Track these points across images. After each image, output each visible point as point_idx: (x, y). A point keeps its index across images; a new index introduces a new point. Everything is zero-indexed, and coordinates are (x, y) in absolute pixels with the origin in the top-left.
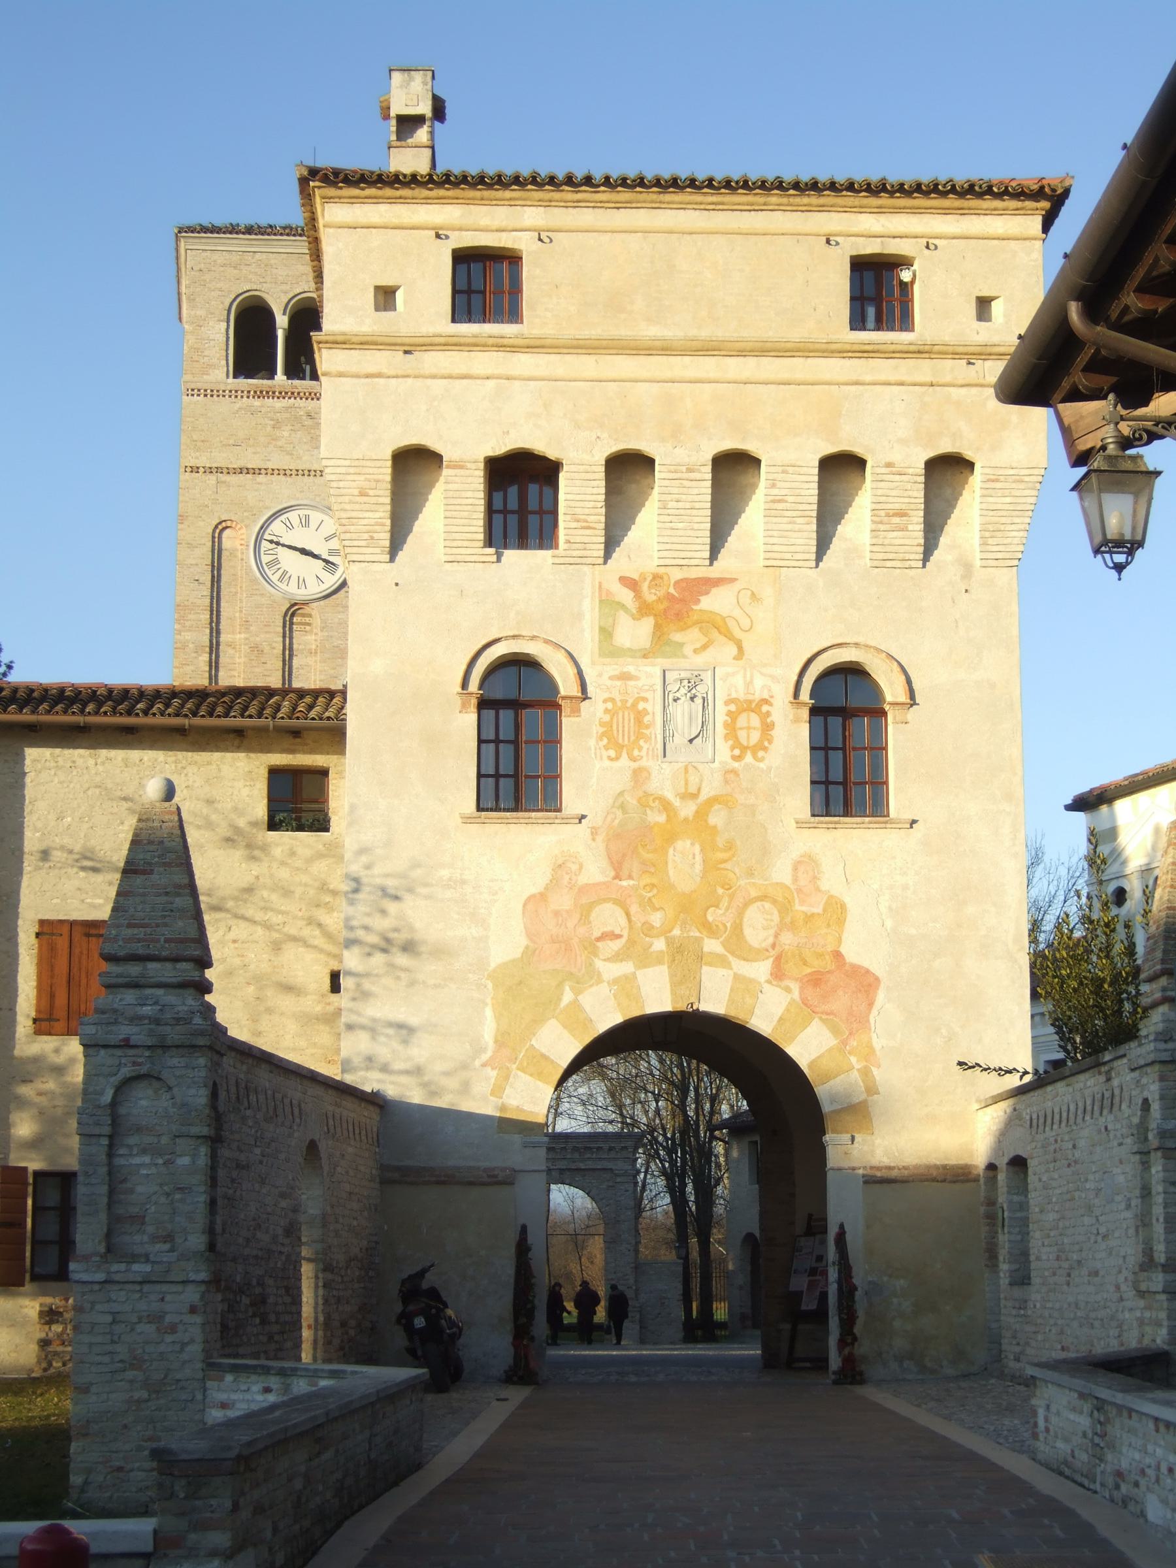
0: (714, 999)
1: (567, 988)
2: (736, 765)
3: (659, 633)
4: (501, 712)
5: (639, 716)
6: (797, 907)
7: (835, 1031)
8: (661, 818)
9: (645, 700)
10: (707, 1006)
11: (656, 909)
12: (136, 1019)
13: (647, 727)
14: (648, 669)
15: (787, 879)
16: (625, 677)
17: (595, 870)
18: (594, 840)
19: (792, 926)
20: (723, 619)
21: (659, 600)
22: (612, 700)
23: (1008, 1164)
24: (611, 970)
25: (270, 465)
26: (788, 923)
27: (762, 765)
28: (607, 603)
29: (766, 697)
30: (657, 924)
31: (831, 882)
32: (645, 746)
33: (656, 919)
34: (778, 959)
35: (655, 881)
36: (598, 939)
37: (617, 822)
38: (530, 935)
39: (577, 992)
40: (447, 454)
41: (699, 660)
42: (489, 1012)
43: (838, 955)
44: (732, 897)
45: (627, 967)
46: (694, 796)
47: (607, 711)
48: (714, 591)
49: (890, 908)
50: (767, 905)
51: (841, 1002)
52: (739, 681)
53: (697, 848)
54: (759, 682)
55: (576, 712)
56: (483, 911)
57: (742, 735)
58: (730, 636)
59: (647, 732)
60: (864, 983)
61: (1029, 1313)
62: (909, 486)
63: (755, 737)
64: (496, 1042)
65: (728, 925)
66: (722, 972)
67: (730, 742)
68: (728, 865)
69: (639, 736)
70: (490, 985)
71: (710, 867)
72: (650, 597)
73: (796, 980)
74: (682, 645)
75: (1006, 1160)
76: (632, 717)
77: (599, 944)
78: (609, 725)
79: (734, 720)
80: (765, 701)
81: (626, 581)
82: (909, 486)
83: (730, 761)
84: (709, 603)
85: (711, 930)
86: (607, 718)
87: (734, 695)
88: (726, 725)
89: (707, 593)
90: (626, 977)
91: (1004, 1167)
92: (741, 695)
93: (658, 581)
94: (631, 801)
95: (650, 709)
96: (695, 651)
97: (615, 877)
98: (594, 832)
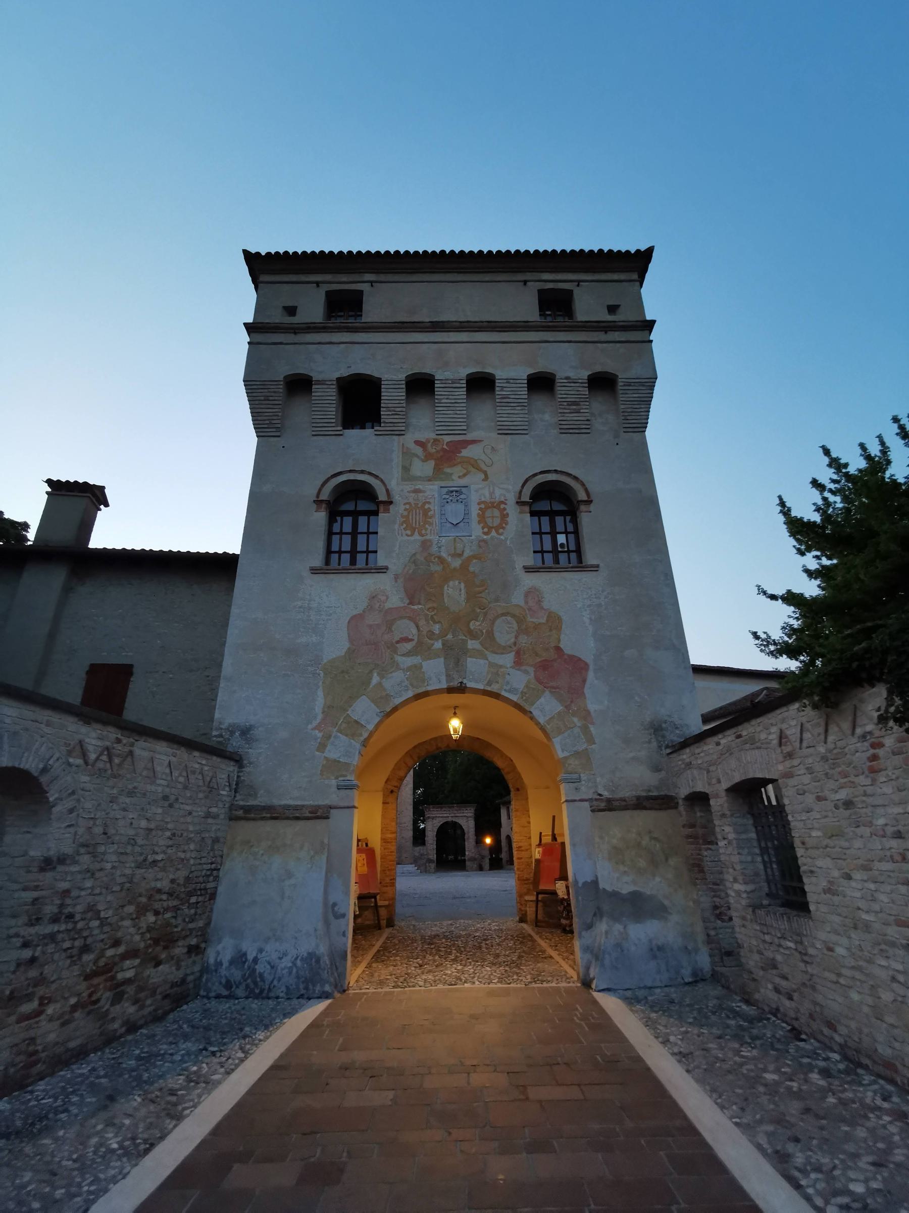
3: (438, 470)
4: (345, 518)
5: (426, 513)
6: (529, 619)
9: (429, 503)
11: (435, 622)
13: (430, 518)
14: (431, 487)
15: (522, 603)
16: (417, 491)
17: (396, 600)
18: (396, 581)
21: (437, 452)
22: (409, 503)
23: (729, 790)
26: (523, 628)
27: (502, 537)
28: (406, 453)
29: (502, 499)
30: (437, 632)
31: (551, 602)
32: (429, 528)
33: (436, 629)
34: (518, 653)
35: (435, 605)
36: (398, 642)
37: (411, 571)
38: (351, 640)
39: (382, 677)
40: (316, 376)
41: (462, 482)
42: (320, 693)
43: (558, 649)
44: (485, 614)
46: (460, 555)
47: (406, 509)
48: (470, 447)
49: (591, 619)
50: (509, 618)
53: (462, 585)
57: (489, 521)
60: (578, 666)
61: (811, 951)
62: (580, 389)
66: (482, 662)
68: (483, 595)
69: (426, 522)
70: (322, 675)
72: (432, 450)
73: (532, 666)
75: (726, 785)
78: (408, 516)
79: (484, 513)
81: (417, 443)
82: (580, 389)
84: (465, 453)
85: (473, 635)
86: (405, 513)
88: (478, 515)
89: (465, 448)
90: (415, 666)
91: (723, 794)
96: (459, 477)
97: (411, 603)
98: (396, 577)
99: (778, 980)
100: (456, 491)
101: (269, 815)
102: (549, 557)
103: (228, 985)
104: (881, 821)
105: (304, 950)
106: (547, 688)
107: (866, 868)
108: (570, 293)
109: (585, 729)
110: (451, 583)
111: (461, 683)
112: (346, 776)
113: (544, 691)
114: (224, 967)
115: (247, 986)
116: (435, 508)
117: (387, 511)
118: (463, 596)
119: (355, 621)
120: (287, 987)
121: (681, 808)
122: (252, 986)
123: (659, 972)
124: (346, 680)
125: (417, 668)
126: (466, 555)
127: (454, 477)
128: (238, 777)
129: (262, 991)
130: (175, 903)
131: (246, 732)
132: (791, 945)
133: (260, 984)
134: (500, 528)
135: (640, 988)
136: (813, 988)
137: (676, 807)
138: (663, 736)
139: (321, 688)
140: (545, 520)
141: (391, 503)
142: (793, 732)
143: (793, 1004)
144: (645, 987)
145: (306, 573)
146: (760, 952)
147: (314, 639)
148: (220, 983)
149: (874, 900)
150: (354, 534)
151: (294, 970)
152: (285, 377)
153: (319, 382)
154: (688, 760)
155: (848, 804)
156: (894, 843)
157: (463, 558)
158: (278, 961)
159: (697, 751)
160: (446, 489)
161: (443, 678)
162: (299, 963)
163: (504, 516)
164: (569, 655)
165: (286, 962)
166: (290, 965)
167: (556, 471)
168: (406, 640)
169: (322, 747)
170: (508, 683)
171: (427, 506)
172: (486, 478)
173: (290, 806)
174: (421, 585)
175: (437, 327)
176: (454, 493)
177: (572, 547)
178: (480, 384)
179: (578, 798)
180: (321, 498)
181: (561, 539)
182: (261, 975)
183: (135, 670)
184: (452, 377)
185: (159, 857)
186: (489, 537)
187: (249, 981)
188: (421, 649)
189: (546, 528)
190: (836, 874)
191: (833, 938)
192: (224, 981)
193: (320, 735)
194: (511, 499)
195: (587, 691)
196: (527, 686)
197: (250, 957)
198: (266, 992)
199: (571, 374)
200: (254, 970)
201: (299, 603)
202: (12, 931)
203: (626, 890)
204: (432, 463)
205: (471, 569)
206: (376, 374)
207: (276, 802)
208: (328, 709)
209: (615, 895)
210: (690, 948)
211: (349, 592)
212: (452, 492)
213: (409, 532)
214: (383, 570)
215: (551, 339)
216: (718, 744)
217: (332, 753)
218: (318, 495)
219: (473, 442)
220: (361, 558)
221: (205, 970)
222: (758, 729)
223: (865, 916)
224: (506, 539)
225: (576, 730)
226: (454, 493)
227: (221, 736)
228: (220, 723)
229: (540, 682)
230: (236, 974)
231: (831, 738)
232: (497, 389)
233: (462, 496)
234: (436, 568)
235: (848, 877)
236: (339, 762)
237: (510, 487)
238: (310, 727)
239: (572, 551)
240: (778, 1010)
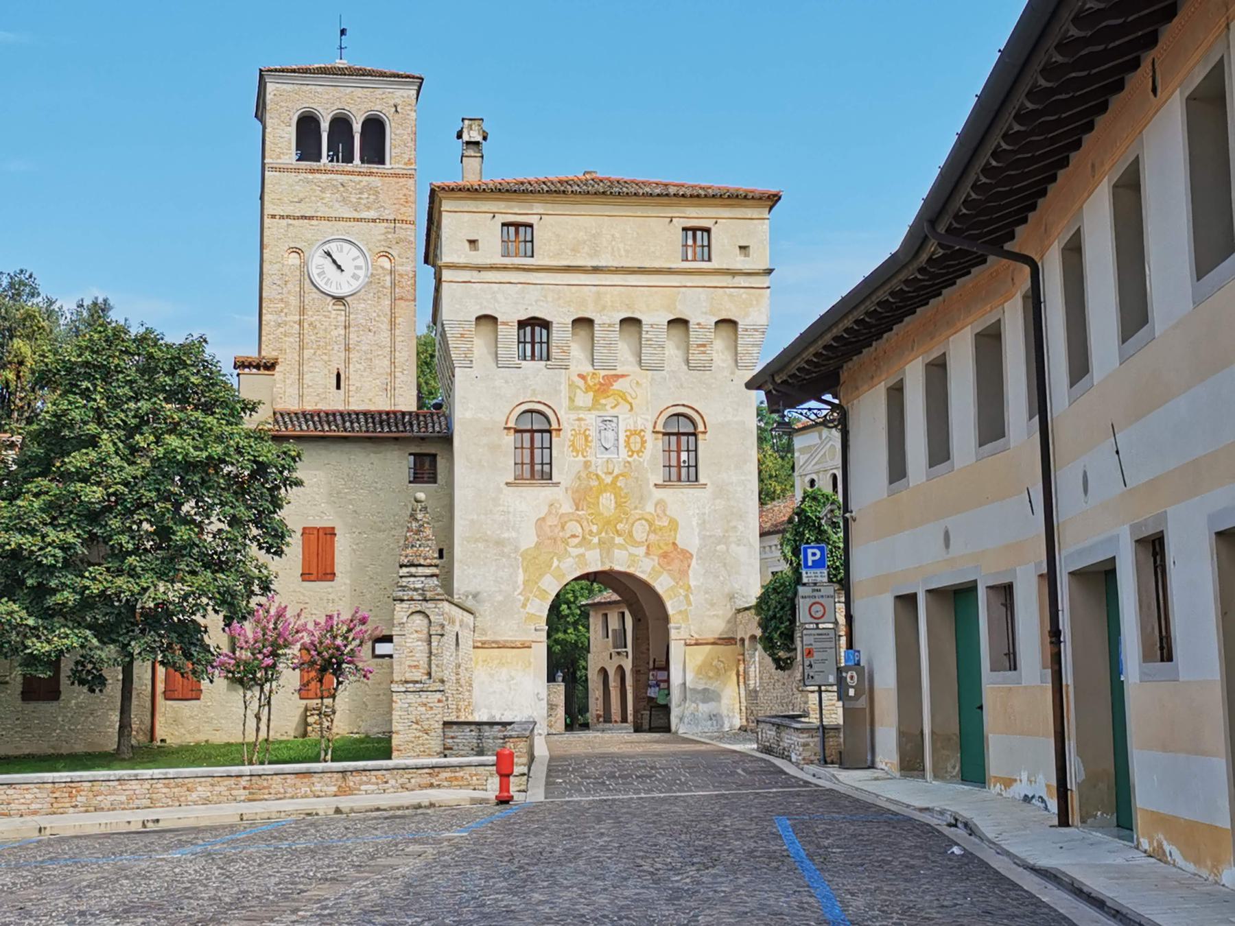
3: (595, 401)
5: (586, 437)
7: (674, 579)
10: (617, 568)
12: (415, 590)
16: (579, 420)
17: (567, 507)
19: (654, 532)
24: (575, 552)
25: (319, 214)
26: (653, 529)
28: (572, 386)
31: (673, 510)
33: (594, 528)
34: (648, 547)
42: (521, 570)
43: (674, 544)
45: (582, 550)
51: (676, 565)
52: (631, 421)
54: (640, 421)
55: (559, 436)
57: (632, 446)
58: (626, 400)
60: (686, 555)
63: (639, 446)
71: (618, 505)
72: (590, 383)
81: (579, 376)
85: (619, 534)
94: (583, 475)
97: (577, 509)
98: (567, 489)
109: (687, 596)
116: (593, 433)
117: (559, 436)
124: (535, 562)
125: (583, 555)
131: (475, 596)
140: (674, 438)
145: (503, 485)
147: (514, 534)
150: (532, 448)
153: (504, 323)
163: (643, 442)
168: (574, 536)
169: (524, 606)
172: (632, 409)
174: (583, 496)
175: (596, 270)
177: (692, 463)
180: (510, 425)
181: (684, 456)
188: (584, 542)
189: (673, 447)
193: (522, 598)
194: (650, 428)
195: (691, 573)
196: (653, 568)
199: (701, 321)
201: (501, 508)
203: (700, 687)
204: (591, 394)
206: (548, 318)
207: (498, 638)
208: (526, 582)
209: (694, 690)
211: (535, 498)
217: (530, 609)
219: (623, 376)
233: (614, 425)
234: (594, 483)
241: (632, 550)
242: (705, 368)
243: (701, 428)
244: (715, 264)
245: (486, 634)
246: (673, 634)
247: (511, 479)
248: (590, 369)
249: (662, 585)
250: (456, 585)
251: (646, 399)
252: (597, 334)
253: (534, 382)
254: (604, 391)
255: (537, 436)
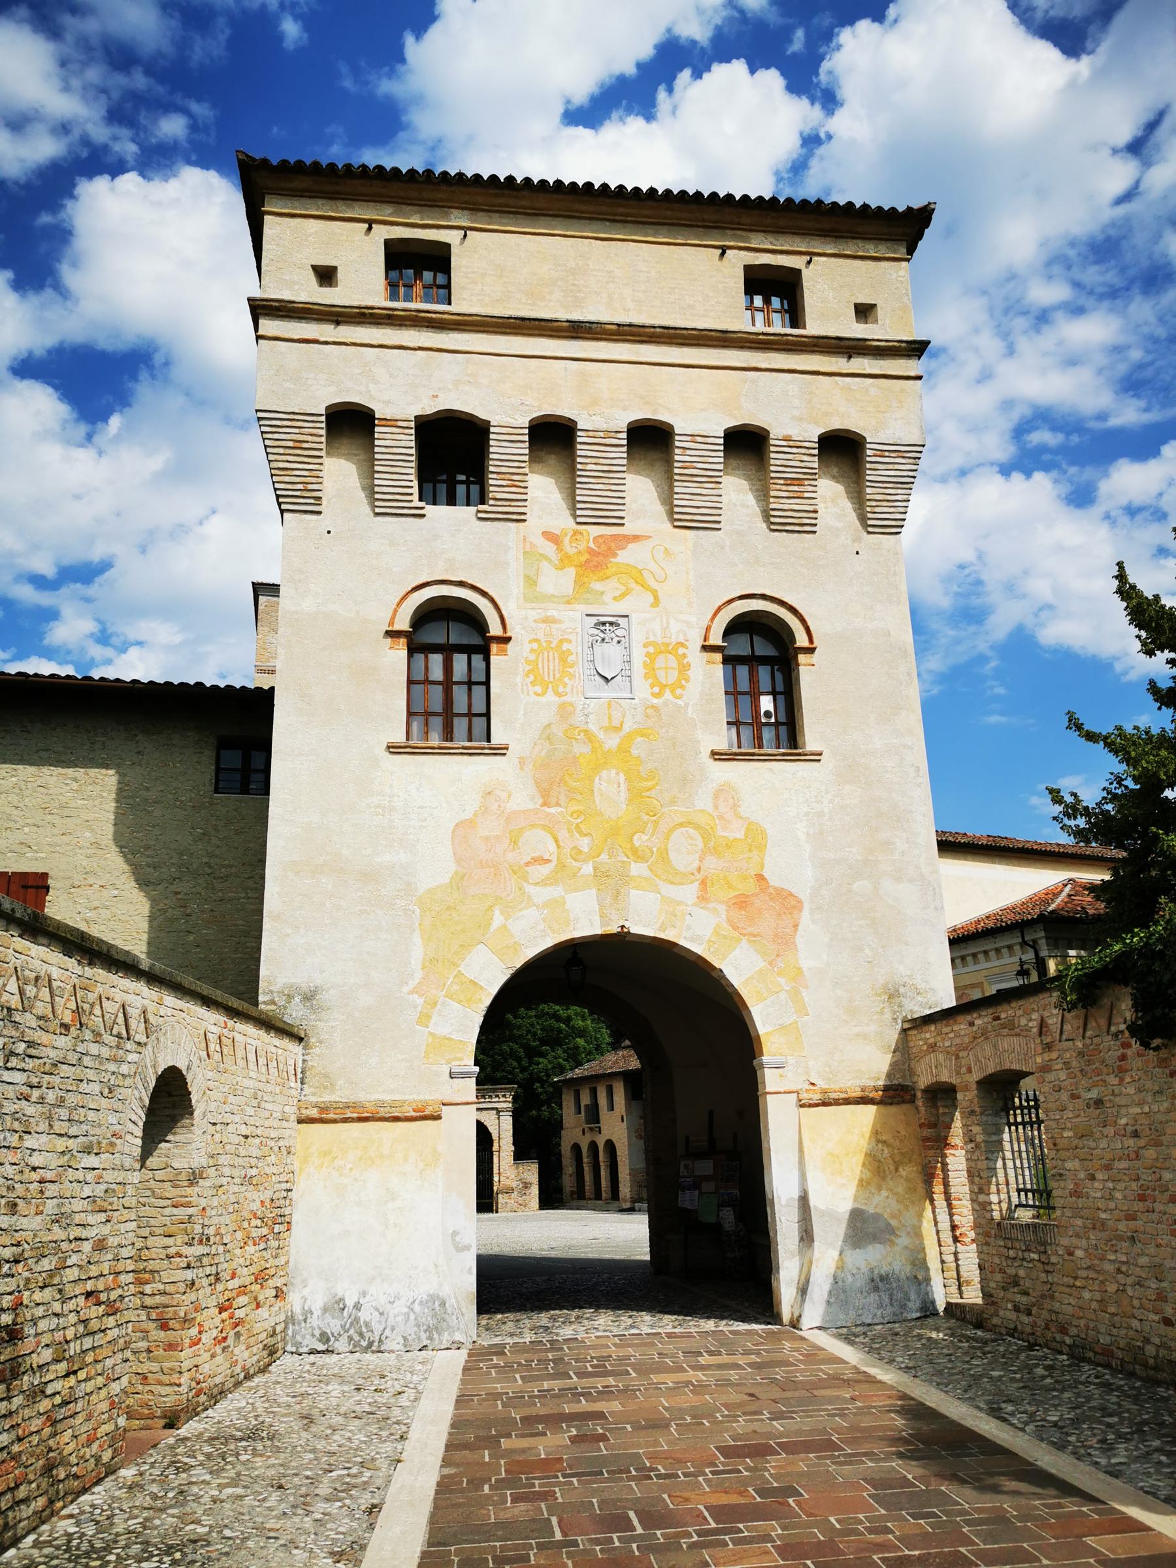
0: (645, 920)
1: (497, 912)
2: (655, 701)
3: (579, 583)
4: (430, 656)
5: (564, 657)
6: (720, 832)
8: (586, 749)
9: (570, 641)
10: (638, 928)
15: (710, 807)
16: (548, 620)
17: (522, 798)
18: (522, 769)
20: (640, 572)
22: (536, 640)
23: (979, 1083)
24: (541, 894)
27: (680, 702)
28: (530, 554)
30: (586, 850)
33: (584, 844)
34: (703, 883)
35: (582, 808)
36: (527, 864)
37: (543, 753)
38: (458, 861)
42: (417, 939)
43: (761, 878)
44: (656, 823)
45: (556, 891)
46: (619, 729)
47: (532, 651)
49: (808, 834)
50: (691, 830)
53: (622, 777)
56: (411, 837)
57: (661, 674)
59: (571, 670)
60: (788, 903)
61: (1054, 1259)
63: (673, 676)
64: (424, 967)
65: (655, 850)
66: (652, 895)
67: (650, 681)
68: (653, 793)
70: (418, 911)
71: (636, 795)
72: (572, 551)
74: (603, 593)
75: (976, 1076)
76: (557, 656)
77: (528, 869)
79: (653, 660)
80: (682, 645)
81: (548, 535)
83: (650, 697)
84: (626, 556)
85: (638, 855)
87: (652, 639)
88: (645, 665)
91: (974, 1086)
92: (660, 640)
93: (578, 537)
95: (573, 650)
96: (615, 598)
97: (545, 804)
98: (522, 762)
99: (1018, 1298)
100: (611, 624)
101: (355, 1115)
102: (746, 732)
103: (324, 1337)
104: (1123, 1121)
105: (423, 1291)
106: (744, 935)
107: (1108, 1167)
108: (796, 274)
110: (604, 773)
111: (623, 927)
112: (462, 1060)
113: (739, 941)
114: (315, 1316)
115: (350, 1338)
117: (504, 653)
118: (622, 794)
119: (463, 829)
120: (405, 1339)
121: (920, 1103)
122: (357, 1338)
123: (880, 1306)
126: (627, 728)
127: (604, 597)
128: (304, 1061)
129: (371, 1344)
130: (265, 1231)
131: (309, 997)
132: (1036, 1256)
133: (367, 1335)
134: (679, 685)
135: (856, 1326)
136: (1052, 1297)
137: (912, 1100)
138: (900, 1006)
139: (417, 931)
140: (743, 671)
141: (508, 639)
142: (1054, 1021)
143: (1031, 1319)
144: (863, 1324)
146: (1002, 1271)
148: (313, 1335)
149: (1112, 1198)
151: (412, 1317)
152: (327, 408)
153: (389, 422)
154: (932, 1040)
155: (1099, 1103)
156: (1131, 1142)
157: (621, 734)
158: (388, 1306)
159: (945, 1030)
160: (594, 620)
161: (597, 918)
162: (417, 1307)
163: (684, 668)
164: (775, 889)
165: (400, 1307)
166: (406, 1310)
167: (763, 597)
168: (541, 861)
169: (424, 1018)
170: (689, 928)
171: (565, 646)
172: (656, 601)
173: (383, 1102)
175: (578, 330)
176: (608, 627)
177: (782, 719)
178: (650, 440)
179: (782, 1090)
180: (397, 627)
182: (367, 1324)
183: (50, 882)
184: (604, 427)
185: (254, 1172)
186: (661, 701)
187: (352, 1332)
188: (562, 874)
189: (744, 685)
190: (1082, 1175)
191: (1074, 1241)
192: (317, 1333)
195: (799, 940)
196: (716, 932)
197: (350, 1303)
198: (376, 1344)
199: (795, 433)
200: (357, 1320)
202: (172, 1251)
204: (571, 572)
205: (635, 752)
206: (482, 414)
210: (920, 1277)
212: (604, 624)
213: (538, 689)
214: (500, 751)
215: (763, 366)
216: (972, 1024)
218: (391, 623)
219: (636, 538)
220: (460, 725)
221: (290, 1320)
222: (1019, 1012)
223: (1103, 1216)
224: (687, 705)
225: (783, 996)
226: (608, 627)
227: (273, 1002)
228: (269, 983)
229: (735, 928)
230: (333, 1325)
231: (1089, 1033)
232: (677, 451)
233: (620, 632)
235: (1092, 1178)
236: (450, 1039)
237: (694, 619)
238: (405, 989)
239: (782, 724)
240: (1015, 1329)
241: (669, 890)
242: (804, 526)
243: (802, 640)
244: (814, 327)
245: (331, 1086)
246: (771, 1080)
247: (399, 737)
248: (570, 523)
249: (739, 968)
250: (263, 972)
251: (691, 568)
252: (581, 450)
253: (450, 545)
254: (599, 567)
255: (460, 662)
